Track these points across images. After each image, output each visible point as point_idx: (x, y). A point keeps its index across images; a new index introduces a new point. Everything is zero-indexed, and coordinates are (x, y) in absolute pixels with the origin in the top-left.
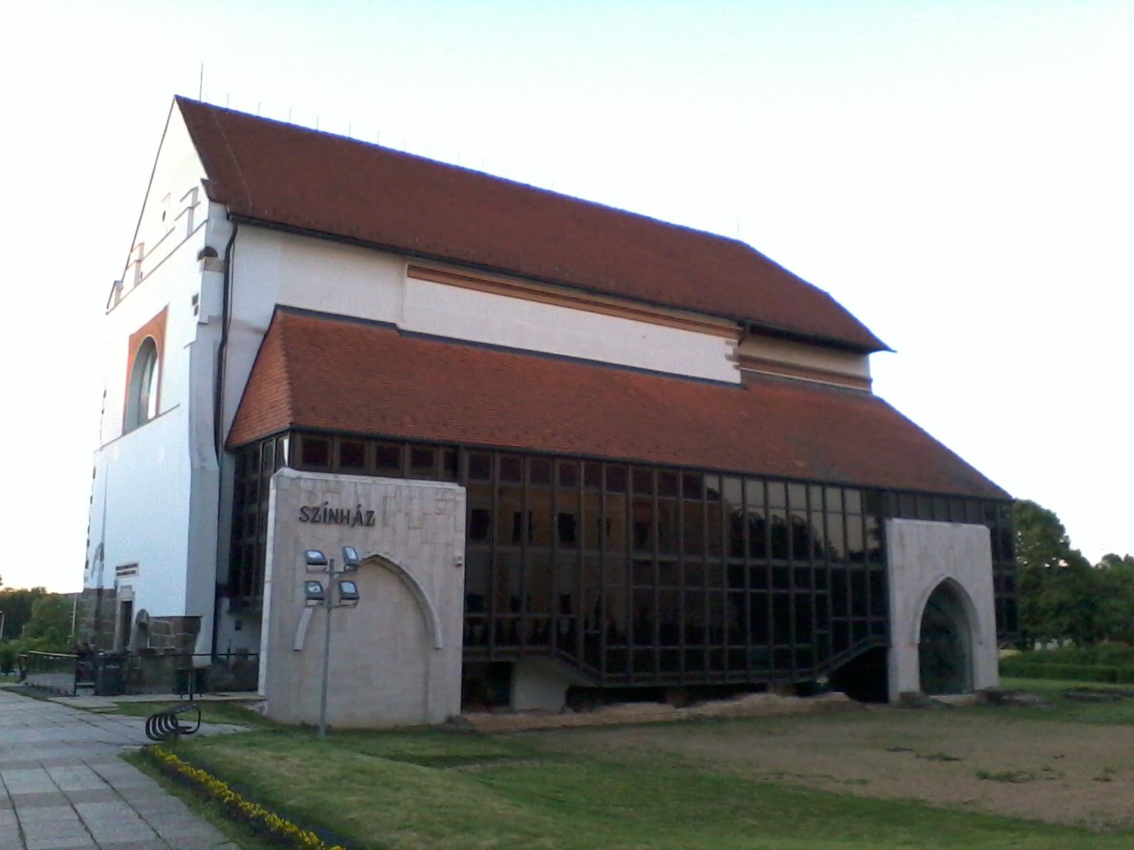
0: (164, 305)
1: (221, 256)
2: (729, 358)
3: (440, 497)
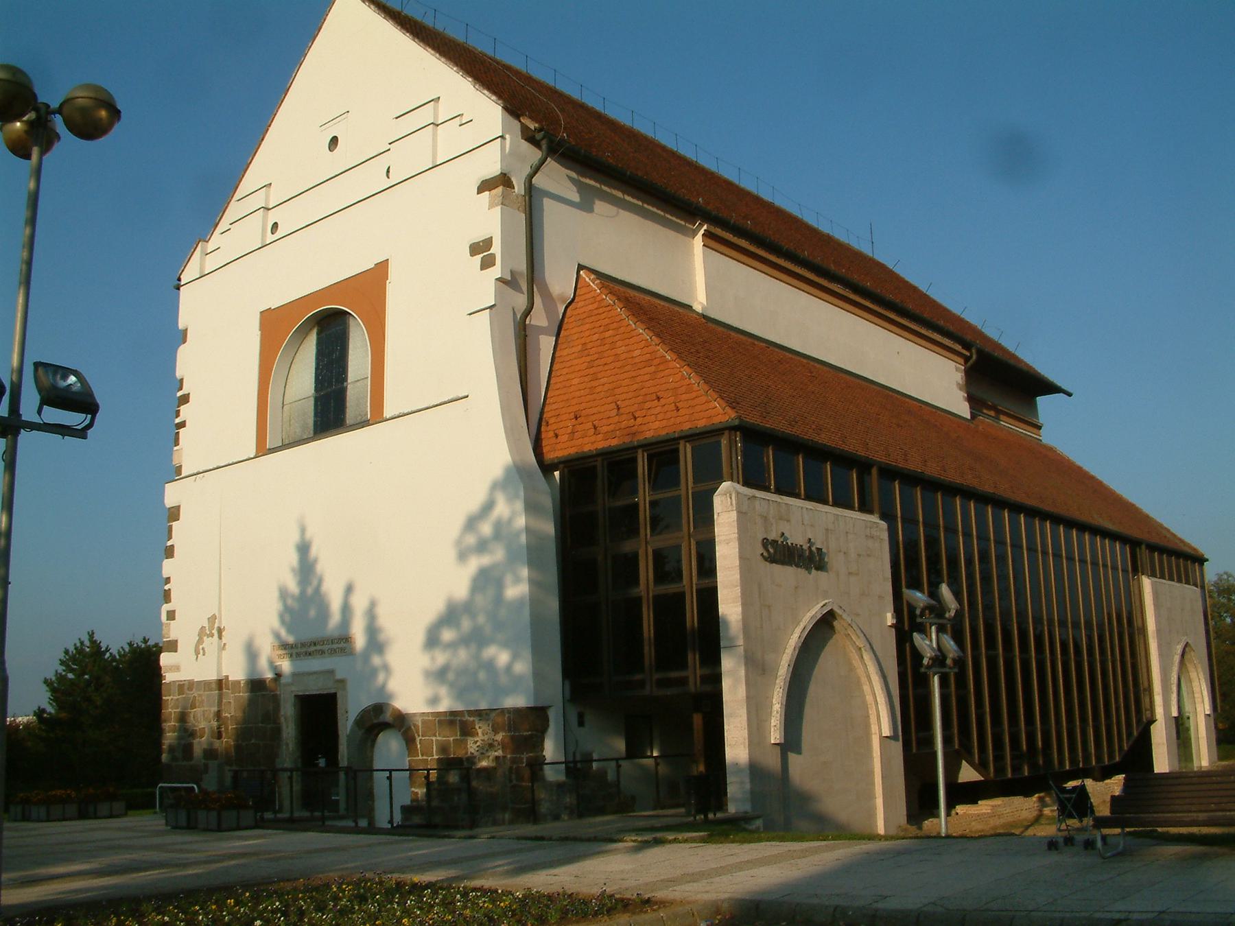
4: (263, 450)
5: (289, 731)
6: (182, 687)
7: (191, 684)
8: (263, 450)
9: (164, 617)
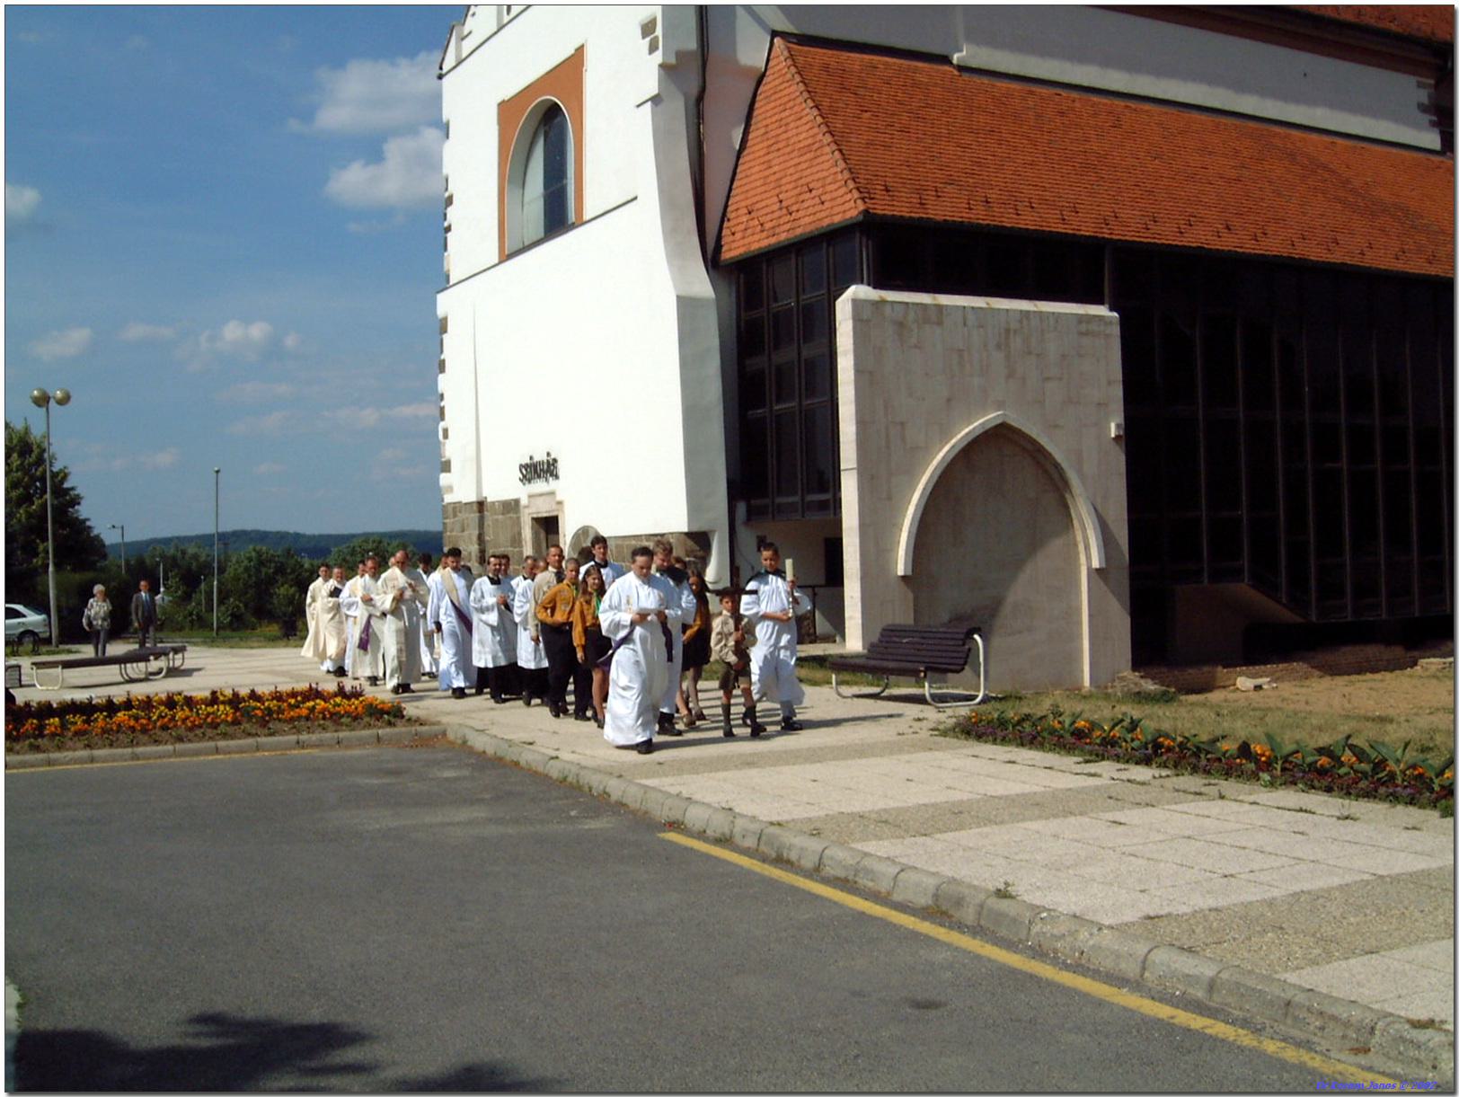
0: (577, 46)
2: (1423, 108)
3: (1083, 327)
8: (506, 256)
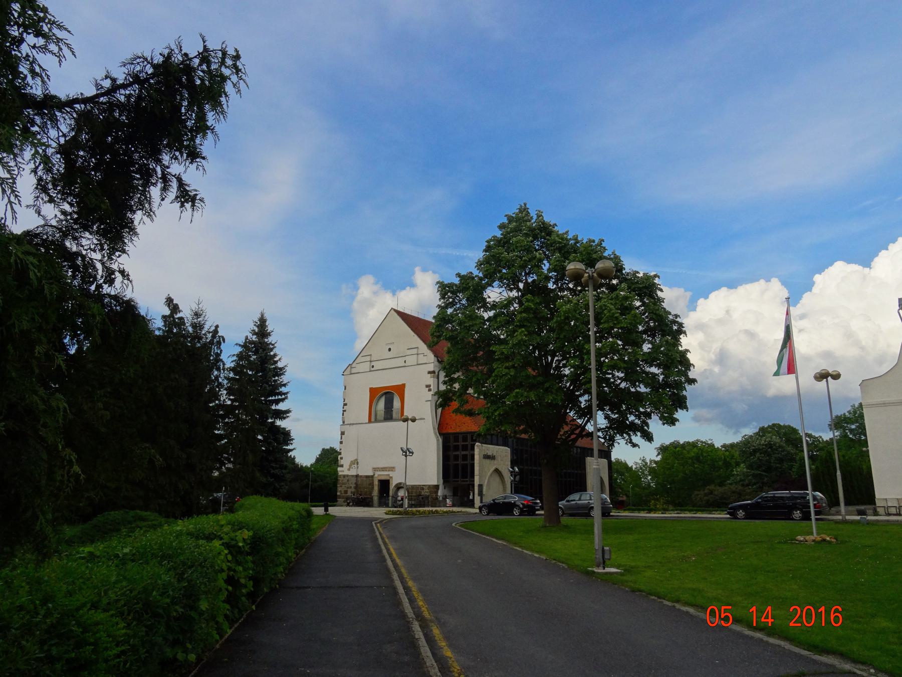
1: (437, 374)
4: (370, 421)
5: (376, 488)
6: (344, 476)
7: (348, 476)
8: (370, 421)
9: (339, 458)
